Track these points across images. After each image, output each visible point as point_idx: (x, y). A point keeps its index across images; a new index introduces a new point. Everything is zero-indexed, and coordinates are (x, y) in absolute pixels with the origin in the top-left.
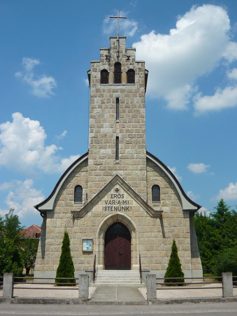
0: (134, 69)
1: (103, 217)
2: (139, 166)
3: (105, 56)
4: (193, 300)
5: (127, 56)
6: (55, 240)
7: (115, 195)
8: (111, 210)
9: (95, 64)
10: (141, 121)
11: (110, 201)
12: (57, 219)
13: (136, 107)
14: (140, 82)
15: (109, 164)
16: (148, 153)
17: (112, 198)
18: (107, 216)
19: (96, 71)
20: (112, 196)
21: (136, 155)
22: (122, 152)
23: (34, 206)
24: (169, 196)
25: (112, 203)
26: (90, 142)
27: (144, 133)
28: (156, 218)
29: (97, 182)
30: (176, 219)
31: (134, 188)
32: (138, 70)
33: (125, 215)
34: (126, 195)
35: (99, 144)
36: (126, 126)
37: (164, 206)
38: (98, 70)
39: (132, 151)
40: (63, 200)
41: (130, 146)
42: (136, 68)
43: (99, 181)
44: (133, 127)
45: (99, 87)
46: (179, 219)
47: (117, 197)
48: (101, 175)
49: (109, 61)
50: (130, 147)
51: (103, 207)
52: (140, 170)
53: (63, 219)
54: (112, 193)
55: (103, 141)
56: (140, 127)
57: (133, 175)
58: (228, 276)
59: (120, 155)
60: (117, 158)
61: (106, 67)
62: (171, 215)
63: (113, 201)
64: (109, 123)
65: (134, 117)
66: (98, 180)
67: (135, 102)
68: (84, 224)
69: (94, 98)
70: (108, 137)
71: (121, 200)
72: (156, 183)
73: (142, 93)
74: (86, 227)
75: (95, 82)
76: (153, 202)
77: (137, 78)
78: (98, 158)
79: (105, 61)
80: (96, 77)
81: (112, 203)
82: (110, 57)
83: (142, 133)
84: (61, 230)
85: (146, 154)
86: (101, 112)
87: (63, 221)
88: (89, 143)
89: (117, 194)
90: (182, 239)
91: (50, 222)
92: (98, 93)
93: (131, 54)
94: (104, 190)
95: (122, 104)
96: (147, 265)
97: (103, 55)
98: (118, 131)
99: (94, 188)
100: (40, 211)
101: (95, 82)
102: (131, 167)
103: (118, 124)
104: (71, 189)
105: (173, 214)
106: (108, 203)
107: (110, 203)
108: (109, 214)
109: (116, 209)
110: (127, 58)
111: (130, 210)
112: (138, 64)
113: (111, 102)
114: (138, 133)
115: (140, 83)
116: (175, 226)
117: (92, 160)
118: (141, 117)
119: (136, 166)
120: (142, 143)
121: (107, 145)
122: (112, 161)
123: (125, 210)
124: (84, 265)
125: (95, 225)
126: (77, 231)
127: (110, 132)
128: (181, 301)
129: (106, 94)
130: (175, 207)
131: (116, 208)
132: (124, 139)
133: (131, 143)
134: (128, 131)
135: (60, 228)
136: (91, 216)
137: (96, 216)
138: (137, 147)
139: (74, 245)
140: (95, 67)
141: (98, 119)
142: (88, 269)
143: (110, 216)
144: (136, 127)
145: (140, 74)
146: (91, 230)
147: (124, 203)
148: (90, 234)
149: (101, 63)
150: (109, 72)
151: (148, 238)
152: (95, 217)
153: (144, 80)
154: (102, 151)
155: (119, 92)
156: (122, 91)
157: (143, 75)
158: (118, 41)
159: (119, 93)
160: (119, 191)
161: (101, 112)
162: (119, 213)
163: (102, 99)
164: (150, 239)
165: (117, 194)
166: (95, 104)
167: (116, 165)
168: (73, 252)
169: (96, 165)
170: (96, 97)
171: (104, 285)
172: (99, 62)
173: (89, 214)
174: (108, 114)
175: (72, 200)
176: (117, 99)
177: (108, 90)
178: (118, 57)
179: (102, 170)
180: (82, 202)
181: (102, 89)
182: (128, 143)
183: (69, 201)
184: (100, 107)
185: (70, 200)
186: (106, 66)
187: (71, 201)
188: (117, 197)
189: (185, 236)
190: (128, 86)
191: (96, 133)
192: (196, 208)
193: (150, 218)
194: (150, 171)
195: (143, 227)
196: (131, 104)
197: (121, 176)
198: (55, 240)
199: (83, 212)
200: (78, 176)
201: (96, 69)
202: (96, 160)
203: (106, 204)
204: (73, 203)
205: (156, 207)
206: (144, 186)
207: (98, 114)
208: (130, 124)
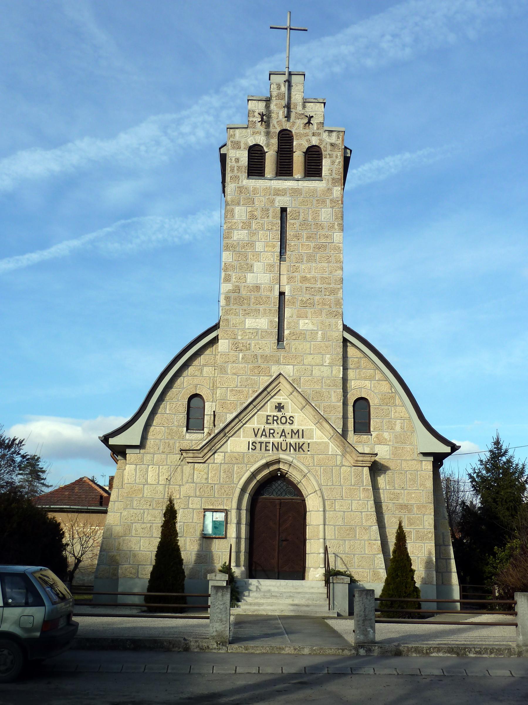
0: (322, 147)
2: (328, 356)
3: (259, 114)
4: (452, 648)
5: (307, 116)
7: (275, 418)
8: (266, 450)
9: (237, 131)
12: (149, 465)
16: (346, 328)
17: (267, 423)
20: (267, 419)
23: (99, 437)
25: (268, 435)
32: (329, 147)
38: (242, 146)
42: (324, 144)
47: (279, 421)
49: (268, 125)
50: (309, 315)
51: (249, 442)
54: (269, 413)
59: (286, 332)
61: (261, 140)
63: (270, 429)
71: (288, 428)
75: (236, 171)
80: (237, 160)
81: (268, 435)
82: (269, 117)
89: (279, 414)
94: (251, 407)
95: (292, 221)
97: (254, 112)
99: (229, 402)
100: (111, 447)
101: (236, 171)
107: (264, 434)
110: (306, 121)
111: (306, 450)
115: (334, 176)
123: (295, 450)
128: (428, 651)
134: (304, 279)
136: (223, 462)
140: (237, 138)
147: (293, 434)
149: (249, 130)
150: (266, 150)
153: (342, 170)
154: (250, 323)
155: (288, 195)
157: (340, 160)
158: (287, 83)
159: (288, 198)
160: (283, 409)
162: (283, 456)
165: (279, 414)
166: (235, 221)
170: (238, 204)
173: (219, 457)
176: (284, 210)
180: (203, 430)
184: (247, 225)
187: (180, 429)
188: (279, 421)
192: (448, 449)
199: (206, 451)
203: (256, 436)
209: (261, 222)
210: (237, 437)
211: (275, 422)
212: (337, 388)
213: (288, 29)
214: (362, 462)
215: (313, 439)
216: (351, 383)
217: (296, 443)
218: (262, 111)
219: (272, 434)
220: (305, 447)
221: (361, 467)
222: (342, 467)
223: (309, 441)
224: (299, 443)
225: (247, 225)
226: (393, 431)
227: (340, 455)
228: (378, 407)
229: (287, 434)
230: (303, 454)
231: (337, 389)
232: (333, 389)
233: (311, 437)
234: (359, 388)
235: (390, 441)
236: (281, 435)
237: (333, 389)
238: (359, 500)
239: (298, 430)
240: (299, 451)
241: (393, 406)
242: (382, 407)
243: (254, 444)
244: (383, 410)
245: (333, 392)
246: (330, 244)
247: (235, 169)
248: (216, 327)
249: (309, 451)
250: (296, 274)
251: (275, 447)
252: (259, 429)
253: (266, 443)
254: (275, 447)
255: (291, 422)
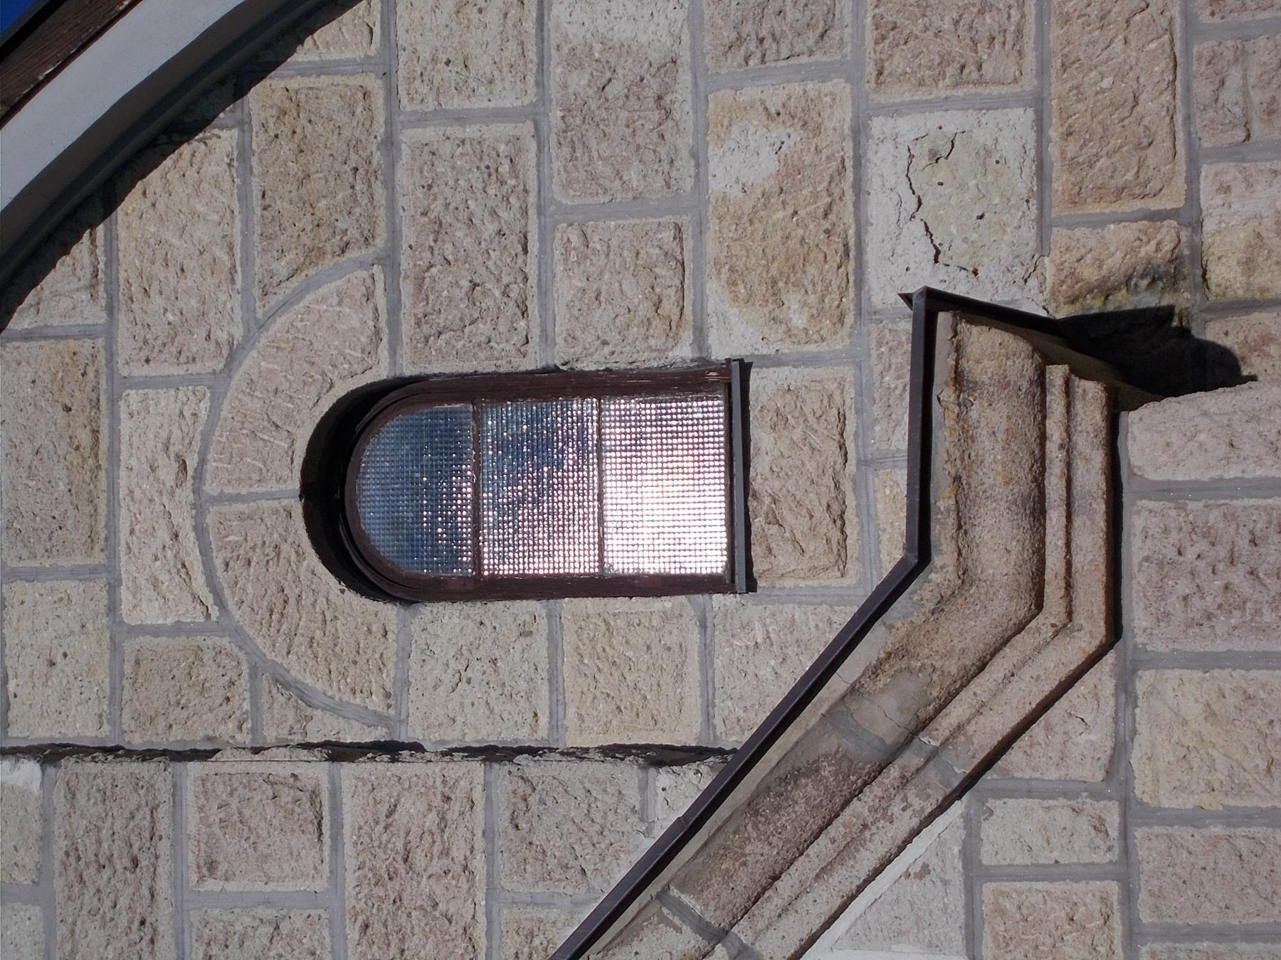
212: (163, 826)
214: (1055, 518)
216: (156, 631)
221: (1137, 520)
222: (1142, 789)
226: (685, 78)
227: (971, 826)
228: (407, 288)
231: (177, 821)
232: (178, 882)
234: (200, 530)
237: (178, 882)
241: (391, 94)
242: (409, 235)
244: (439, 228)
245: (212, 885)
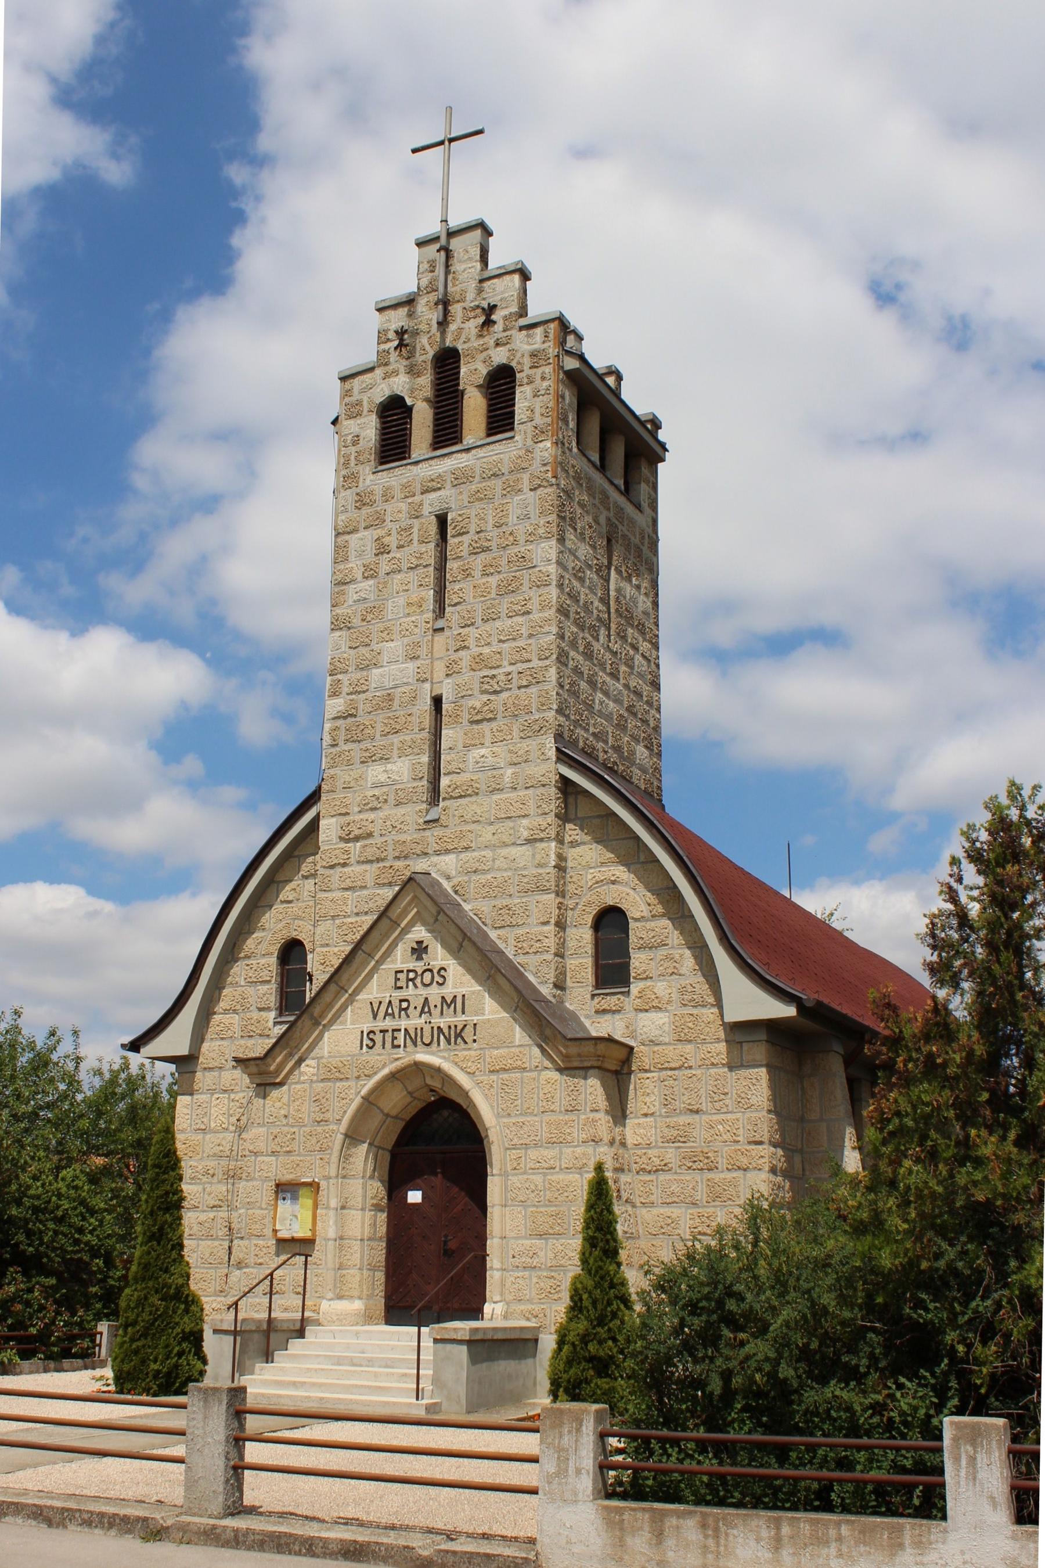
0: (513, 364)
1: (358, 1077)
2: (525, 822)
3: (396, 332)
6: (204, 1190)
7: (412, 975)
10: (534, 605)
11: (390, 1002)
12: (212, 1094)
13: (515, 542)
14: (537, 415)
15: (400, 831)
18: (375, 1073)
19: (359, 414)
20: (397, 979)
21: (509, 772)
22: (452, 767)
24: (669, 958)
26: (327, 739)
27: (547, 662)
28: (582, 1073)
29: (349, 920)
30: (698, 1072)
31: (499, 932)
32: (527, 362)
33: (447, 1067)
34: (455, 970)
35: (363, 745)
36: (471, 642)
37: (646, 1011)
38: (366, 407)
39: (495, 755)
40: (235, 1012)
41: (488, 734)
42: (519, 355)
43: (357, 914)
44: (500, 641)
45: (368, 482)
46: (713, 1071)
47: (418, 981)
48: (365, 887)
51: (362, 1032)
52: (530, 841)
53: (232, 1096)
54: (399, 966)
55: (379, 727)
56: (531, 636)
57: (499, 869)
58: (206, 1401)
59: (444, 781)
60: (435, 795)
61: (400, 384)
62: (672, 1053)
63: (401, 1001)
64: (406, 640)
65: (507, 589)
66: (355, 911)
67: (512, 519)
68: (286, 1116)
69: (347, 537)
70: (396, 703)
71: (434, 993)
72: (610, 898)
73: (545, 468)
74: (293, 1126)
75: (353, 462)
76: (593, 996)
77: (523, 401)
78: (356, 809)
79: (394, 356)
83: (541, 663)
84: (224, 1143)
85: (559, 760)
86: (372, 597)
87: (232, 1104)
88: (324, 744)
89: (419, 966)
90: (729, 1175)
91: (185, 1111)
92: (366, 511)
93: (503, 292)
95: (456, 540)
96: (537, 1308)
98: (440, 669)
99: (336, 950)
101: (353, 462)
102: (487, 834)
103: (439, 638)
104: (263, 961)
105: (689, 1048)
106: (381, 1014)
108: (384, 1066)
109: (414, 1038)
110: (482, 319)
111: (469, 1040)
112: (531, 332)
113: (415, 541)
114: (520, 667)
115: (539, 420)
116: (695, 1107)
117: (334, 820)
118: (538, 587)
119: (511, 824)
120: (538, 710)
121: (392, 744)
122: (412, 813)
123: (449, 1041)
124: (283, 1302)
125: (328, 1115)
126: (261, 1146)
127: (405, 680)
129: (397, 509)
130: (695, 1011)
131: (413, 1036)
132: (463, 702)
133: (490, 720)
134: (480, 661)
135: (221, 1136)
136: (315, 1078)
137: (333, 1075)
138: (516, 733)
139: (250, 1212)
141: (361, 629)
142: (222, 1321)
143: (386, 1071)
144: (514, 639)
145: (538, 377)
146: (314, 1140)
147: (445, 1007)
148: (309, 1158)
149: (379, 372)
151: (545, 1174)
152: (329, 1080)
154: (376, 773)
155: (448, 485)
156: (460, 479)
161: (372, 597)
162: (423, 1056)
163: (380, 532)
164: (554, 1178)
165: (419, 966)
167: (428, 833)
168: (241, 1242)
169: (347, 841)
171: (263, 1395)
172: (371, 369)
173: (308, 1068)
174: (401, 601)
175: (268, 1009)
176: (442, 521)
177: (404, 487)
178: (443, 324)
179: (371, 862)
181: (378, 491)
182: (479, 717)
183: (255, 1015)
184: (370, 573)
185: (260, 1009)
186: (396, 379)
188: (418, 980)
189: (744, 1161)
190: (484, 449)
191: (354, 696)
193: (555, 1075)
194: (584, 843)
195: (521, 1119)
196: (496, 532)
197: (448, 878)
198: (204, 1190)
200: (290, 898)
201: (359, 403)
202: (348, 819)
203: (375, 1016)
204: (271, 1024)
205: (608, 1017)
206: (541, 920)
207: (362, 606)
208: (488, 627)
209: (398, 556)
210: (342, 1023)
211: (411, 983)
213: (447, 143)
215: (483, 1014)
217: (450, 1027)
218: (401, 324)
219: (406, 1009)
220: (468, 1034)
222: (544, 1073)
223: (475, 1019)
224: (456, 1026)
225: (370, 573)
229: (432, 1008)
230: (464, 1049)
233: (480, 1011)
235: (669, 1002)
236: (422, 1012)
238: (576, 1147)
239: (455, 997)
240: (456, 1043)
243: (371, 1036)
246: (530, 571)
247: (352, 458)
248: (314, 798)
249: (475, 1041)
250: (462, 653)
251: (411, 1038)
252: (380, 1003)
253: (394, 1030)
254: (411, 1038)
255: (441, 981)
